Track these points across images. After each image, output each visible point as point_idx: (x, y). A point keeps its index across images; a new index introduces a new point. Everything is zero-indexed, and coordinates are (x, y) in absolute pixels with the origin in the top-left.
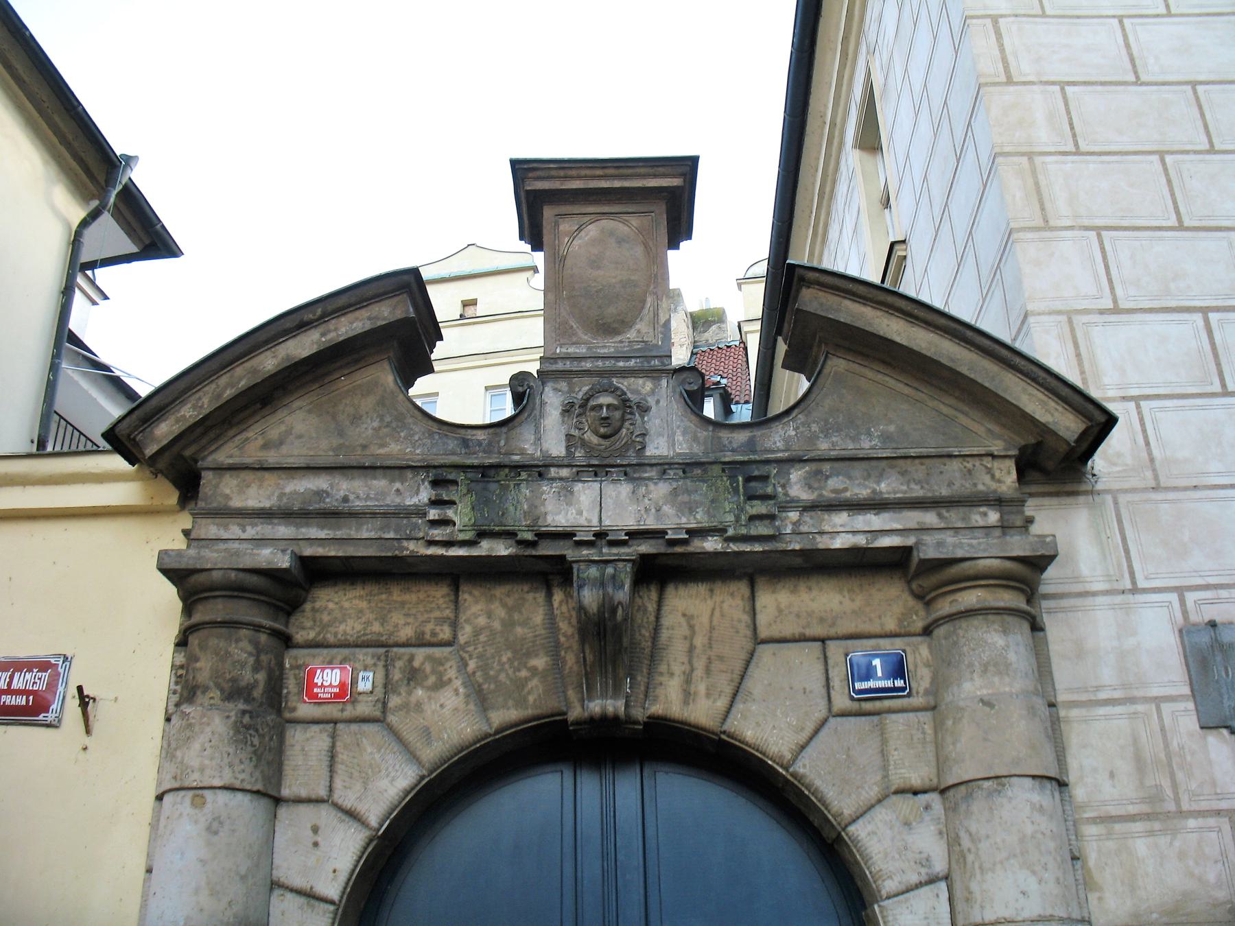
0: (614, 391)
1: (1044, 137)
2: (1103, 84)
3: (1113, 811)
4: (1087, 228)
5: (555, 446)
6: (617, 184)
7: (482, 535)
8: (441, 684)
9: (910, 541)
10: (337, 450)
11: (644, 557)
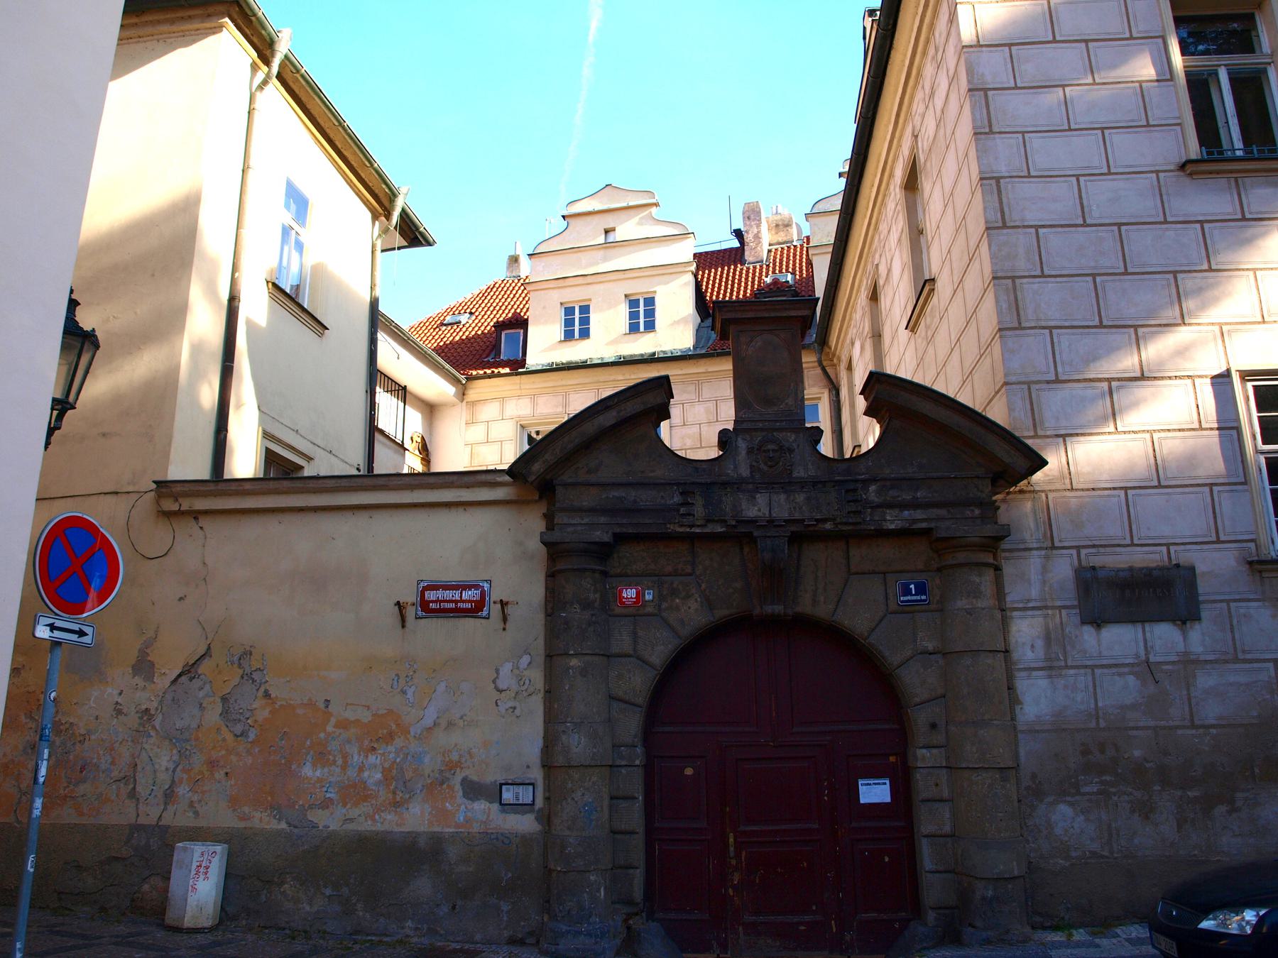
1: (1022, 265)
2: (1062, 226)
3: (1033, 665)
4: (1044, 328)
5: (745, 472)
6: (773, 315)
7: (708, 521)
8: (688, 597)
9: (933, 525)
11: (792, 532)
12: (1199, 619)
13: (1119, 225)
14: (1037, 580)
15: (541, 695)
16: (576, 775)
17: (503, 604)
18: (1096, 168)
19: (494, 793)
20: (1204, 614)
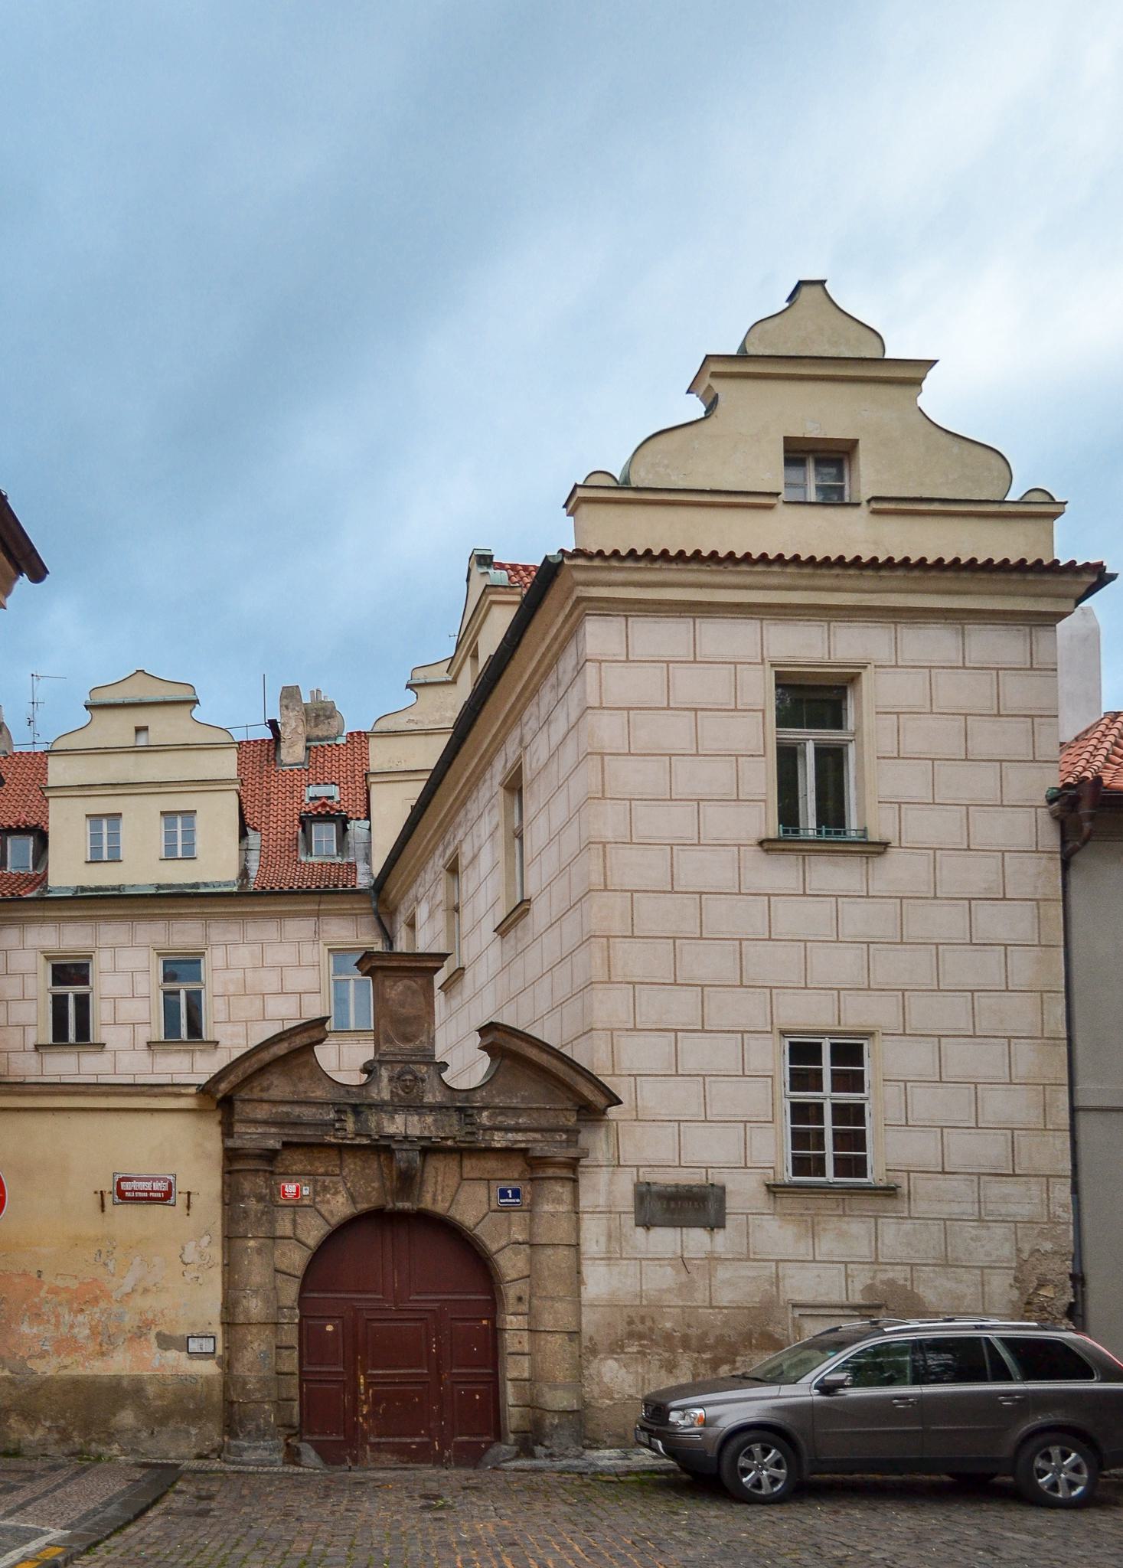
0: (411, 1072)
5: (386, 1096)
6: (414, 964)
7: (357, 1135)
8: (336, 1193)
10: (294, 1093)
12: (724, 1227)
13: (701, 893)
14: (607, 1189)
15: (219, 1269)
16: (254, 1330)
17: (189, 1193)
18: (687, 838)
19: (183, 1343)
20: (728, 1223)
